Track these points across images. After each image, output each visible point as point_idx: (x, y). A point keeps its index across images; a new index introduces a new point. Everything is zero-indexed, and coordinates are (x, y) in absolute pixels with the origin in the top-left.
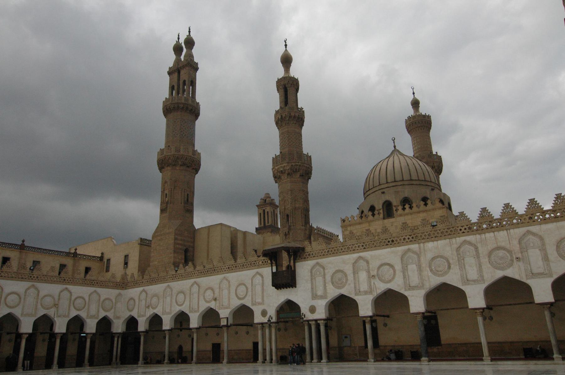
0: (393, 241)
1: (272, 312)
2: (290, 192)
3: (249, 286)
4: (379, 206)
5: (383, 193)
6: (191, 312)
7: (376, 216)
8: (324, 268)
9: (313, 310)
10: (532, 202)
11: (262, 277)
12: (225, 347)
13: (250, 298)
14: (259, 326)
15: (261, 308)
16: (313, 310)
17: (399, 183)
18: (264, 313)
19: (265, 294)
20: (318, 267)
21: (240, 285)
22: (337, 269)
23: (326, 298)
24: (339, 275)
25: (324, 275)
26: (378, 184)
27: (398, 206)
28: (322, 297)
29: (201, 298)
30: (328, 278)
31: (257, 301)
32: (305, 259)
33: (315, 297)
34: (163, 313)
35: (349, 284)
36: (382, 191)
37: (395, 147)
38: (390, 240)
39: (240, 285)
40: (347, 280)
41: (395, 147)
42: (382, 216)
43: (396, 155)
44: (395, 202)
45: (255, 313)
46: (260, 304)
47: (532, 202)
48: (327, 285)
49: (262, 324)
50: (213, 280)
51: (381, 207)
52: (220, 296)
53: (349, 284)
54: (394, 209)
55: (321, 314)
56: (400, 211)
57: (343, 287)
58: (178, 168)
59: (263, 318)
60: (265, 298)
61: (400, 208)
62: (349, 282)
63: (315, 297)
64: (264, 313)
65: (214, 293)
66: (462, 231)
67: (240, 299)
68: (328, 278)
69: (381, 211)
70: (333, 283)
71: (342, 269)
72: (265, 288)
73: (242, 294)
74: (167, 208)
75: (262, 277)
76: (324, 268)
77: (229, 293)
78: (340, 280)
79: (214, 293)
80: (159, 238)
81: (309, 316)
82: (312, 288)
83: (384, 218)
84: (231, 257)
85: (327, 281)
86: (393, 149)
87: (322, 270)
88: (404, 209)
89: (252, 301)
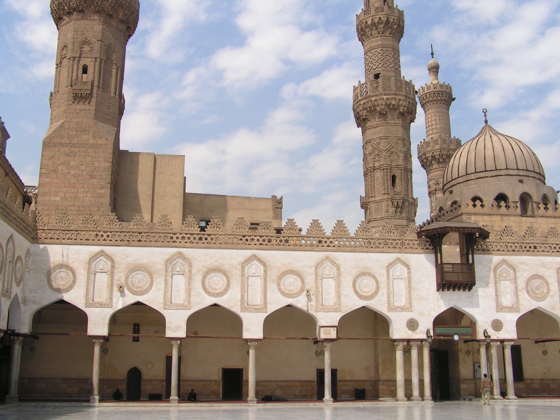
0: (535, 247)
1: (426, 325)
2: (401, 142)
3: (383, 279)
4: (514, 196)
5: (521, 181)
6: (244, 309)
7: (512, 210)
8: (514, 269)
9: (497, 325)
10: (340, 223)
11: (408, 267)
12: (251, 377)
13: (385, 299)
14: (400, 346)
15: (408, 316)
16: (497, 325)
17: (531, 174)
18: (412, 325)
19: (414, 294)
20: (504, 266)
21: (362, 274)
22: (535, 273)
23: (518, 312)
24: (536, 283)
25: (515, 278)
26: (504, 167)
27: (539, 203)
28: (511, 309)
29: (272, 287)
30: (521, 283)
31: (396, 304)
32: (486, 251)
33: (500, 308)
34: (165, 304)
35: (552, 296)
36: (522, 178)
37: (486, 122)
38: (532, 245)
39: (362, 274)
40: (548, 291)
41: (486, 122)
42: (519, 211)
43: (488, 133)
44: (536, 197)
45: (244, 323)
46: (402, 309)
47: (340, 223)
48: (519, 293)
49: (409, 341)
50: (154, 255)
51: (517, 199)
52: (317, 288)
53: (552, 296)
54: (535, 206)
55: (509, 332)
56: (542, 211)
57: (543, 298)
58: (114, 24)
59: (410, 332)
60: (414, 302)
61: (542, 206)
62: (551, 293)
63: (500, 308)
64: (412, 325)
65: (303, 282)
66: (207, 241)
67: (361, 297)
68: (521, 283)
69: (518, 204)
70: (528, 292)
71: (541, 274)
72: (413, 285)
73: (365, 290)
74: (91, 94)
75: (408, 267)
76: (514, 269)
77: (338, 286)
78: (537, 289)
79: (303, 282)
80: (66, 149)
81: (494, 335)
82: (497, 296)
83: (521, 216)
84: (113, 216)
85: (519, 288)
86: (484, 124)
87: (511, 271)
88: (546, 208)
89: (389, 304)
